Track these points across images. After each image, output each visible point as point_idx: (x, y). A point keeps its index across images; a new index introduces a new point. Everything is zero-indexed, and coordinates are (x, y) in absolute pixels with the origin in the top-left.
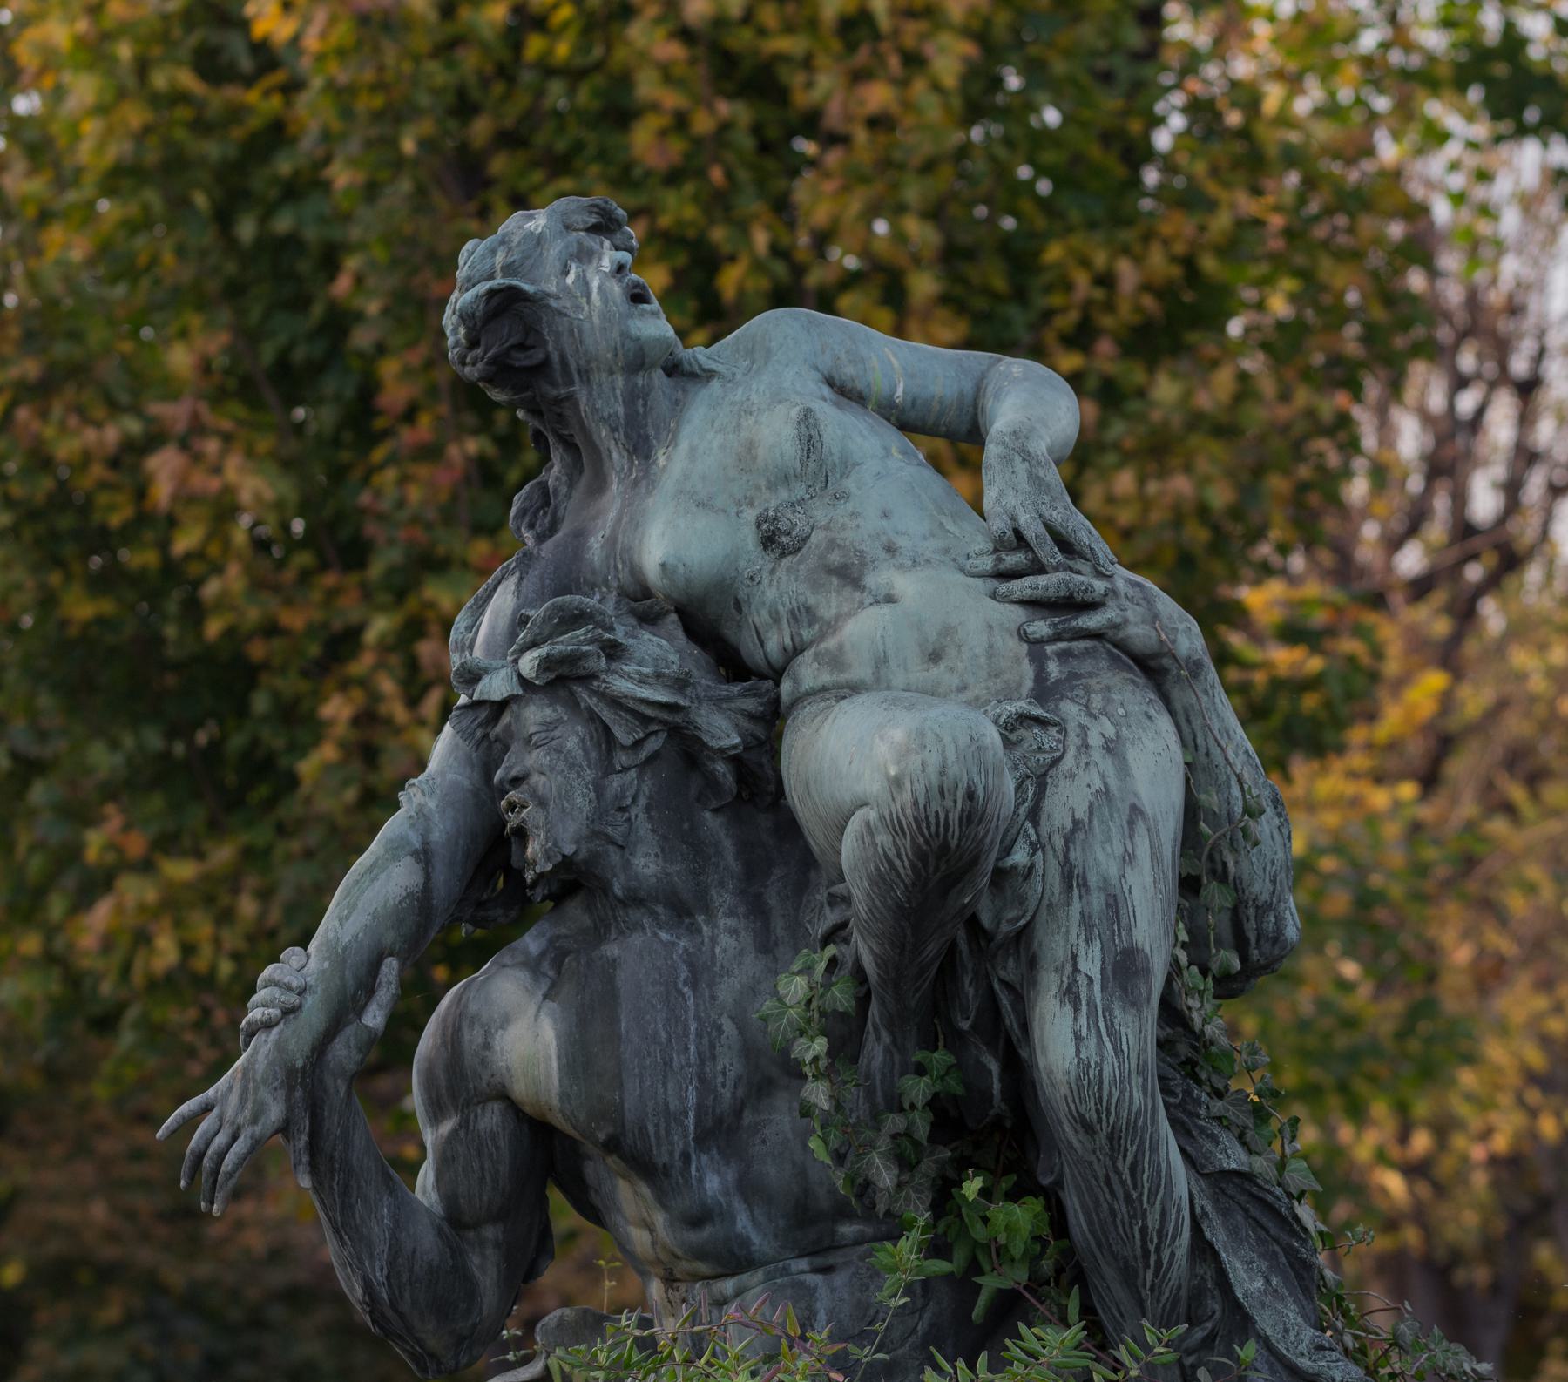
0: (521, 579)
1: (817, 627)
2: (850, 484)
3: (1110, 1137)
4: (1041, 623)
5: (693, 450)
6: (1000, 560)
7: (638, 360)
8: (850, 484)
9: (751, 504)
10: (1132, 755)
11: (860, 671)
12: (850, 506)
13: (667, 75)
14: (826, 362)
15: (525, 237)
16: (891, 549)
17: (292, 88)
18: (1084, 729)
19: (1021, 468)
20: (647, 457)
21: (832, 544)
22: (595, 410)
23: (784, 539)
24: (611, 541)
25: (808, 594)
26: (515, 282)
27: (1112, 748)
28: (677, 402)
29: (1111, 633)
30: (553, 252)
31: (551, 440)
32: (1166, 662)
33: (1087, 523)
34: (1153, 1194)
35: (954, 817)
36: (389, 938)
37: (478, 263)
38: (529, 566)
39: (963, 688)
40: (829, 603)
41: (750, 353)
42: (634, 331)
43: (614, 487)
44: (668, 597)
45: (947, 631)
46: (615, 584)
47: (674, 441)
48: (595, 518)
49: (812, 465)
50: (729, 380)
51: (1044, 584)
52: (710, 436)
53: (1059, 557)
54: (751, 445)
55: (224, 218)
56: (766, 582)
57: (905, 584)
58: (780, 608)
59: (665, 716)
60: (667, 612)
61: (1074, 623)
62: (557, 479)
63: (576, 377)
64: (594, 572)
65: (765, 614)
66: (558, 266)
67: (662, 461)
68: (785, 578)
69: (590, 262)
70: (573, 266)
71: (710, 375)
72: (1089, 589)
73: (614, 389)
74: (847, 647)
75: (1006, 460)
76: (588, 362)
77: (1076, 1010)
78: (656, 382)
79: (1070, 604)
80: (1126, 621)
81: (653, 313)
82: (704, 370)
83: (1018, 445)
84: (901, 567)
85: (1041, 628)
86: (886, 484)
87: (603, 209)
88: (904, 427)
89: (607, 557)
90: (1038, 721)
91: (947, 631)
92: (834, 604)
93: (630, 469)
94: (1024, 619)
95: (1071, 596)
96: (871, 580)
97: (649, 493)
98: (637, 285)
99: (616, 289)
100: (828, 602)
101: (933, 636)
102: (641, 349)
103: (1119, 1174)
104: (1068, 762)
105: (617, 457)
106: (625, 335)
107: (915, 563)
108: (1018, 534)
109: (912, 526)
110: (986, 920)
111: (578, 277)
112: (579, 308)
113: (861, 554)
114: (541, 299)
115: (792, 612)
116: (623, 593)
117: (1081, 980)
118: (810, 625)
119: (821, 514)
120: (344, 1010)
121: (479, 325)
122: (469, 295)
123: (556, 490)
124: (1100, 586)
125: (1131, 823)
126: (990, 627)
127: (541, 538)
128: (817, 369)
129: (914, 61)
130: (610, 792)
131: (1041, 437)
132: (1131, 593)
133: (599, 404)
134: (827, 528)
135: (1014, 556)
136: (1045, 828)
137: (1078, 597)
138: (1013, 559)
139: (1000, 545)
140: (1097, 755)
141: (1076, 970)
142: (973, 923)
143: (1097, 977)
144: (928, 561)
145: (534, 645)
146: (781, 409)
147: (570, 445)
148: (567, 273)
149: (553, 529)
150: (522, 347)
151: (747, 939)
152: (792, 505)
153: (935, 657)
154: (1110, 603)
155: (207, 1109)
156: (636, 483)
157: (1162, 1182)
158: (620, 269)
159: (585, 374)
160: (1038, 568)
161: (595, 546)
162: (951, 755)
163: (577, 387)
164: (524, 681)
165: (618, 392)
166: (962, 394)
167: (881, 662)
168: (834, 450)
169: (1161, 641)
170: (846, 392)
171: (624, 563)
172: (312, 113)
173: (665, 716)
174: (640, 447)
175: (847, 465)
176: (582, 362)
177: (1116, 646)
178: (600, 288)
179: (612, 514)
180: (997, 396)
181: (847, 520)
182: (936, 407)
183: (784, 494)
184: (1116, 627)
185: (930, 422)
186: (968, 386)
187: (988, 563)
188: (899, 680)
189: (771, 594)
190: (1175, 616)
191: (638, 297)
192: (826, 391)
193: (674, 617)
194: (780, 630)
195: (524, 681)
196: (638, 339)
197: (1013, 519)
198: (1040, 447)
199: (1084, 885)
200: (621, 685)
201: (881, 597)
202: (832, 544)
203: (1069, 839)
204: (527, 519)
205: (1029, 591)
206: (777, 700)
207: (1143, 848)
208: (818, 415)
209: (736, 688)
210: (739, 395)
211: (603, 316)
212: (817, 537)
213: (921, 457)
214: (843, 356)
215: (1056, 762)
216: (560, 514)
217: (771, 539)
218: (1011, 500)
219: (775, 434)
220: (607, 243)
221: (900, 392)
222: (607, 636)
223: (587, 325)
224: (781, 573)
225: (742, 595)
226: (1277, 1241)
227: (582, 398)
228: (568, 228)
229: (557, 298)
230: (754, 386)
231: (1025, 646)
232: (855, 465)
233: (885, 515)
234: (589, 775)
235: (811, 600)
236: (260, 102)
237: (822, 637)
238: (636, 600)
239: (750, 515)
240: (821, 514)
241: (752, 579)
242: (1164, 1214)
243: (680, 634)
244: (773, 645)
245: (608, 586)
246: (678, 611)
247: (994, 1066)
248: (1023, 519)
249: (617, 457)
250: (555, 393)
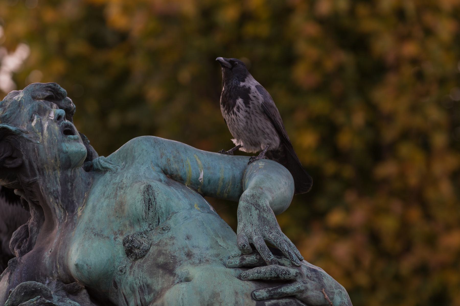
0: (11, 273)
1: (152, 294)
2: (171, 223)
4: (263, 291)
5: (94, 207)
6: (243, 259)
7: (68, 163)
8: (171, 223)
9: (122, 234)
12: (170, 234)
13: (313, 41)
14: (163, 162)
15: (12, 103)
16: (189, 255)
17: (131, 52)
19: (255, 213)
20: (73, 211)
21: (160, 253)
22: (47, 189)
23: (137, 251)
24: (54, 254)
25: (148, 278)
26: (5, 126)
28: (89, 184)
29: (299, 295)
30: (26, 110)
31: (30, 204)
33: (289, 240)
38: (15, 267)
40: (158, 283)
41: (125, 159)
42: (64, 149)
43: (57, 228)
44: (81, 281)
46: (56, 275)
47: (86, 203)
48: (48, 242)
49: (151, 214)
50: (115, 172)
51: (264, 271)
52: (102, 200)
53: (273, 257)
54: (121, 205)
55: (103, 115)
56: (128, 272)
57: (196, 272)
58: (135, 285)
60: (81, 289)
61: (279, 290)
62: (32, 224)
63: (37, 172)
64: (46, 269)
65: (128, 288)
66: (28, 117)
67: (79, 213)
68: (137, 270)
69: (45, 115)
70: (36, 117)
71: (106, 170)
72: (288, 273)
73: (56, 178)
74: (166, 304)
75: (248, 209)
76: (42, 165)
78: (78, 174)
80: (307, 289)
81: (76, 140)
82: (103, 168)
83: (254, 201)
84: (193, 264)
85: (263, 293)
86: (189, 223)
87: (54, 89)
88: (205, 194)
89: (52, 262)
91: (215, 295)
92: (160, 283)
93: (65, 218)
94: (254, 288)
95: (278, 277)
96: (179, 271)
97: (72, 229)
98: (67, 126)
99: (56, 128)
100: (158, 282)
101: (207, 298)
102: (69, 157)
105: (58, 212)
106: (60, 151)
107: (200, 261)
108: (252, 245)
109: (201, 243)
111: (37, 122)
112: (37, 138)
113: (174, 257)
114: (19, 134)
115: (140, 287)
116: (60, 280)
118: (149, 294)
119: (155, 238)
123: (31, 229)
124: (293, 271)
126: (236, 293)
127: (22, 254)
128: (158, 166)
129: (429, 32)
131: (267, 198)
132: (310, 275)
133: (49, 185)
134: (158, 245)
135: (250, 258)
137: (282, 277)
138: (250, 259)
139: (244, 252)
144: (207, 261)
146: (136, 186)
147: (38, 207)
148: (32, 120)
149: (30, 248)
150: (11, 158)
152: (141, 234)
154: (299, 280)
156: (67, 225)
158: (59, 118)
159: (41, 170)
160: (262, 263)
161: (47, 255)
163: (38, 177)
165: (58, 179)
166: (234, 177)
168: (163, 206)
169: (325, 299)
170: (173, 177)
171: (60, 265)
172: (139, 64)
174: (70, 207)
175: (170, 213)
176: (39, 165)
177: (302, 301)
178: (48, 127)
179: (55, 241)
180: (250, 178)
181: (168, 241)
182: (221, 184)
183: (137, 229)
184: (302, 292)
185: (219, 191)
186: (237, 173)
187: (237, 261)
189: (130, 279)
190: (333, 286)
191: (67, 132)
192: (162, 176)
193: (85, 291)
194: (135, 296)
196: (67, 152)
197: (250, 238)
198: (266, 202)
201: (183, 279)
202: (160, 253)
204: (18, 244)
205: (256, 275)
208: (154, 189)
210: (118, 179)
211: (51, 142)
212: (153, 250)
213: (212, 209)
214: (172, 159)
216: (33, 241)
218: (250, 229)
219: (134, 199)
220: (55, 105)
221: (201, 176)
222: (47, 301)
223: (41, 146)
224: (135, 268)
225: (117, 279)
227: (41, 182)
228: (34, 98)
229: (27, 133)
230: (125, 175)
231: (255, 302)
232: (174, 213)
233: (188, 238)
235: (149, 281)
236: (116, 57)
237: (154, 300)
238: (66, 283)
239: (120, 239)
240: (155, 238)
241: (121, 271)
243: (88, 300)
245: (52, 276)
246: (86, 288)
248: (255, 238)
249: (58, 212)
250: (27, 180)
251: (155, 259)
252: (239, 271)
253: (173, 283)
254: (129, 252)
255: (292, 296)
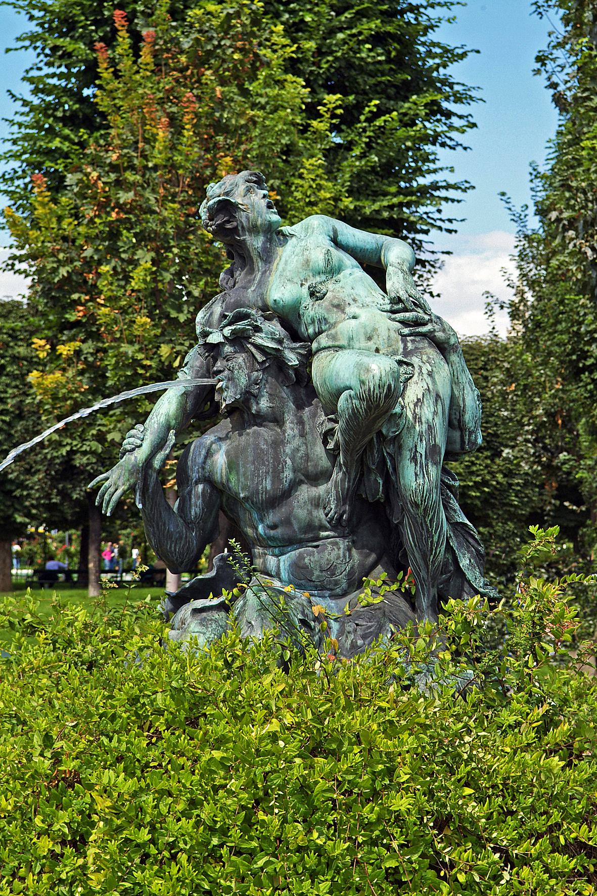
3: (424, 510)
5: (286, 261)
10: (436, 377)
11: (343, 342)
12: (340, 284)
16: (354, 300)
18: (420, 368)
21: (335, 297)
27: (430, 374)
32: (446, 345)
34: (436, 530)
35: (383, 395)
36: (173, 422)
37: (214, 190)
39: (377, 350)
40: (333, 317)
45: (375, 330)
59: (273, 353)
77: (416, 465)
79: (418, 323)
84: (358, 307)
85: (406, 331)
90: (406, 363)
91: (375, 330)
96: (347, 310)
103: (426, 522)
104: (415, 378)
110: (384, 431)
117: (418, 454)
120: (158, 446)
121: (213, 213)
122: (211, 202)
124: (427, 317)
125: (436, 401)
130: (253, 378)
136: (406, 401)
140: (425, 376)
141: (416, 451)
142: (380, 433)
143: (424, 454)
145: (230, 324)
151: (296, 431)
153: (370, 339)
155: (107, 479)
157: (439, 526)
160: (405, 310)
162: (383, 374)
164: (225, 337)
167: (351, 339)
173: (273, 353)
187: (388, 307)
188: (357, 345)
195: (225, 337)
199: (420, 421)
200: (259, 341)
202: (335, 297)
203: (416, 405)
206: (311, 350)
207: (440, 407)
209: (298, 345)
215: (411, 378)
217: (313, 294)
218: (397, 285)
226: (473, 546)
234: (246, 371)
237: (330, 329)
242: (439, 537)
244: (311, 331)
247: (381, 482)
251: (331, 301)
252: (390, 314)
253: (344, 319)
254: (312, 294)
255: (423, 335)
